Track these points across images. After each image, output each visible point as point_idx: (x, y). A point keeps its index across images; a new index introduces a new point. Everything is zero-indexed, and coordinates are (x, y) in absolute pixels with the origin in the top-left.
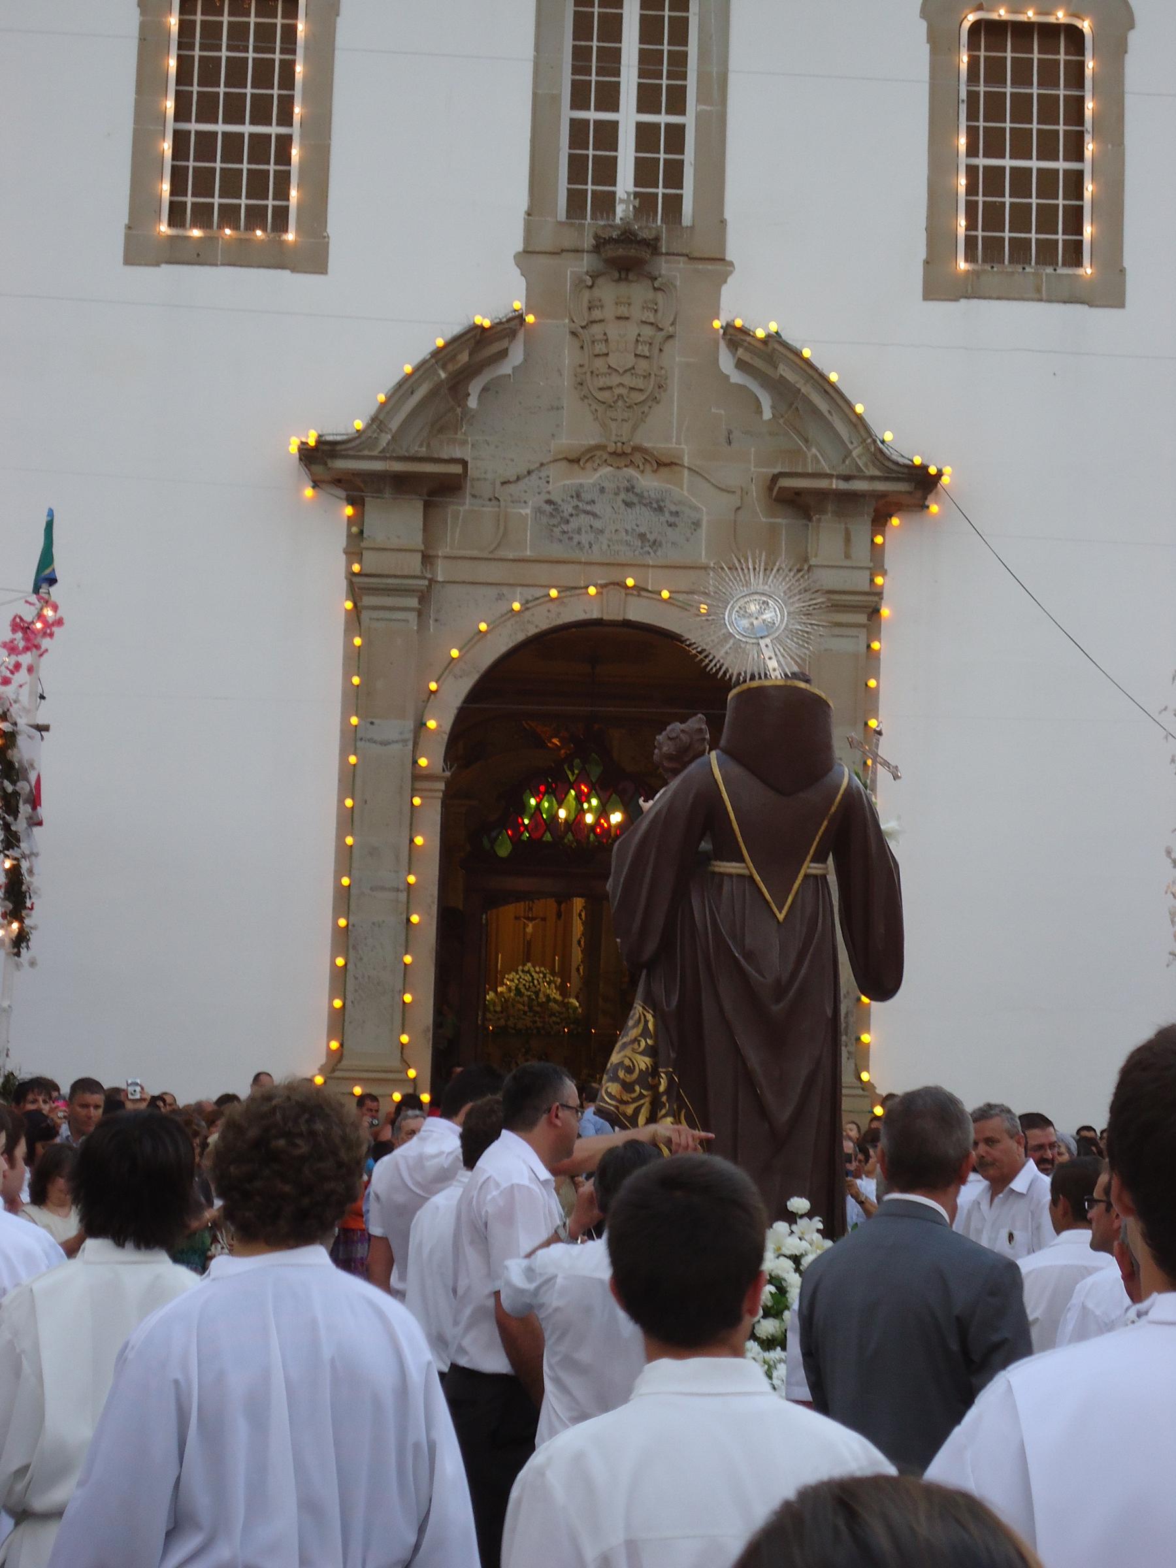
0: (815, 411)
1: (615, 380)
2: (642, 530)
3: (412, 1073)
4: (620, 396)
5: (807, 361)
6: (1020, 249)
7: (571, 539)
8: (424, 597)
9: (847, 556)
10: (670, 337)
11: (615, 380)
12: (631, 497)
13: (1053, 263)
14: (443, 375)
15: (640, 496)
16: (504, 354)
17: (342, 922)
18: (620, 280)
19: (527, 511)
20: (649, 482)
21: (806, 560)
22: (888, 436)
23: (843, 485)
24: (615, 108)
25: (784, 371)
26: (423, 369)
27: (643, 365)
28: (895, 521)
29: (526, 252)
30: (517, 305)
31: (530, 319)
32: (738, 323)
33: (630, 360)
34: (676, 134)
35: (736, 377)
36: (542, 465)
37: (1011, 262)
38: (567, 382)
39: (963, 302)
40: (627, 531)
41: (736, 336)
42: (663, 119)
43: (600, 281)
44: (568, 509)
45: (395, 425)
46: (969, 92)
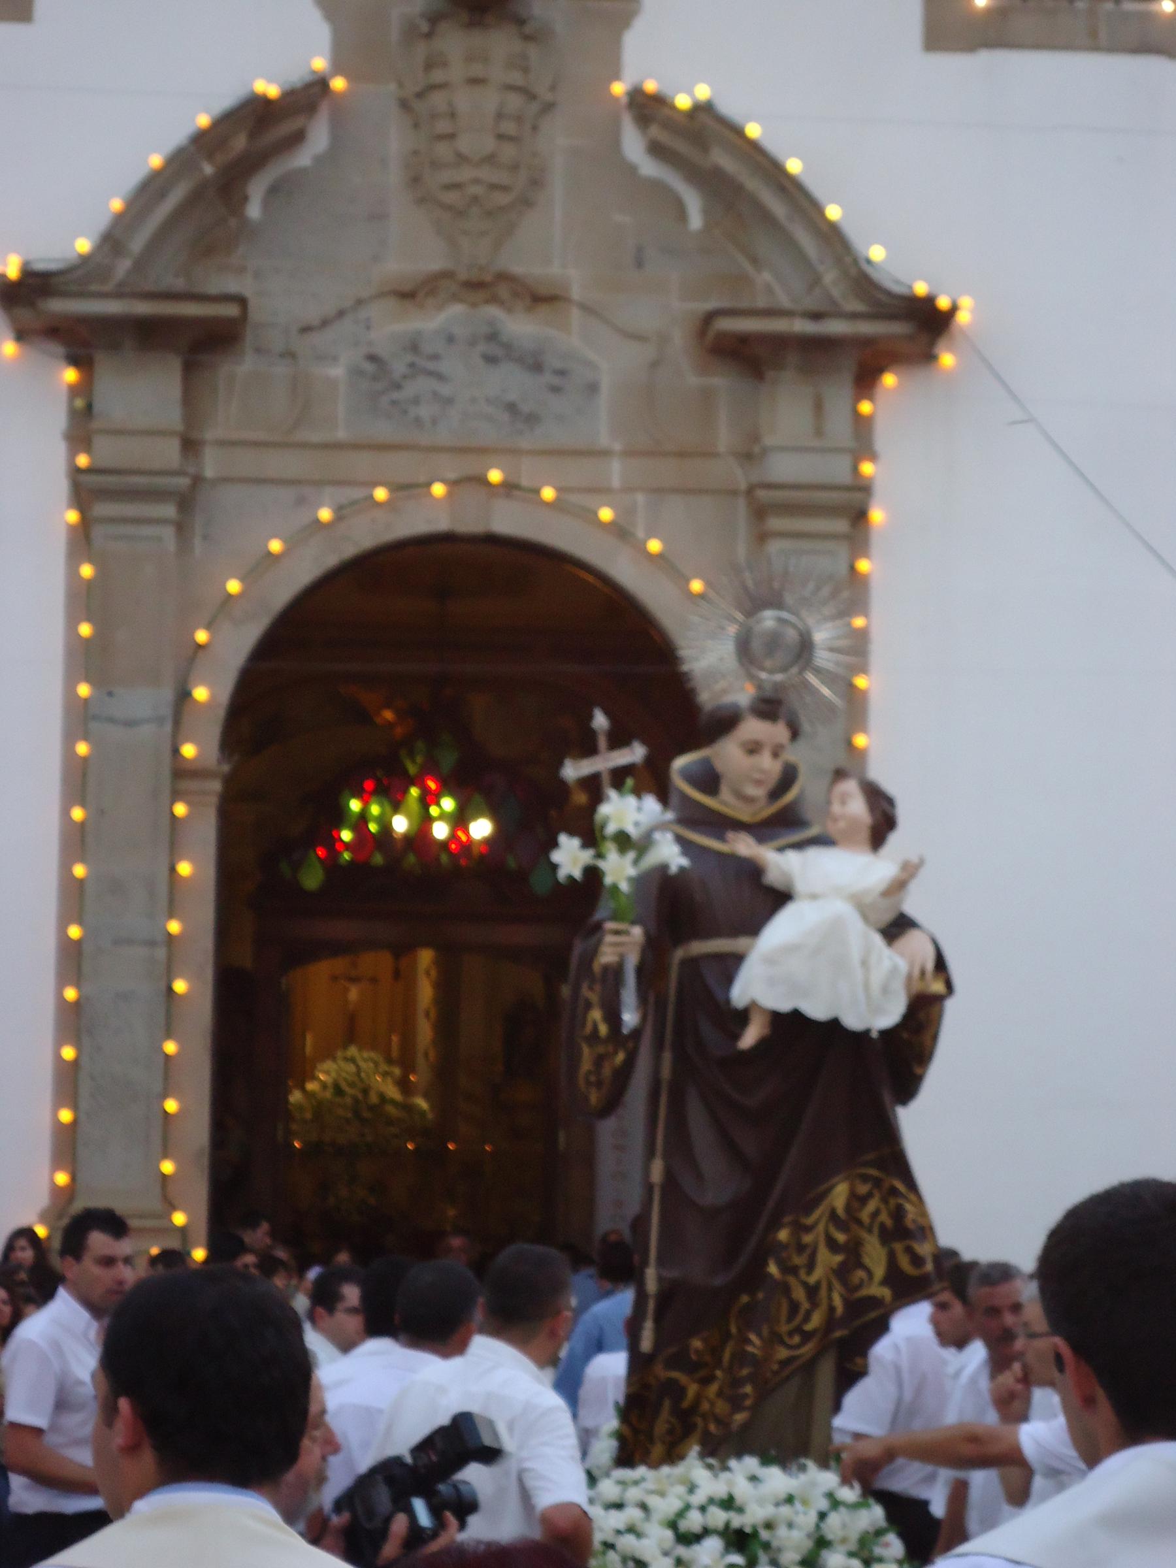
0: (766, 218)
1: (465, 174)
2: (512, 396)
3: (179, 1219)
4: (475, 199)
5: (754, 145)
7: (405, 412)
8: (186, 502)
9: (819, 432)
10: (549, 107)
11: (465, 174)
12: (494, 350)
15: (508, 347)
16: (297, 138)
17: (71, 994)
18: (471, 25)
19: (337, 372)
21: (755, 437)
22: (877, 253)
26: (179, 162)
27: (508, 152)
28: (889, 380)
30: (319, 64)
31: (338, 84)
32: (650, 86)
33: (489, 144)
35: (649, 167)
36: (360, 302)
38: (394, 177)
40: (488, 400)
43: (443, 26)
44: (399, 367)
45: (138, 243)
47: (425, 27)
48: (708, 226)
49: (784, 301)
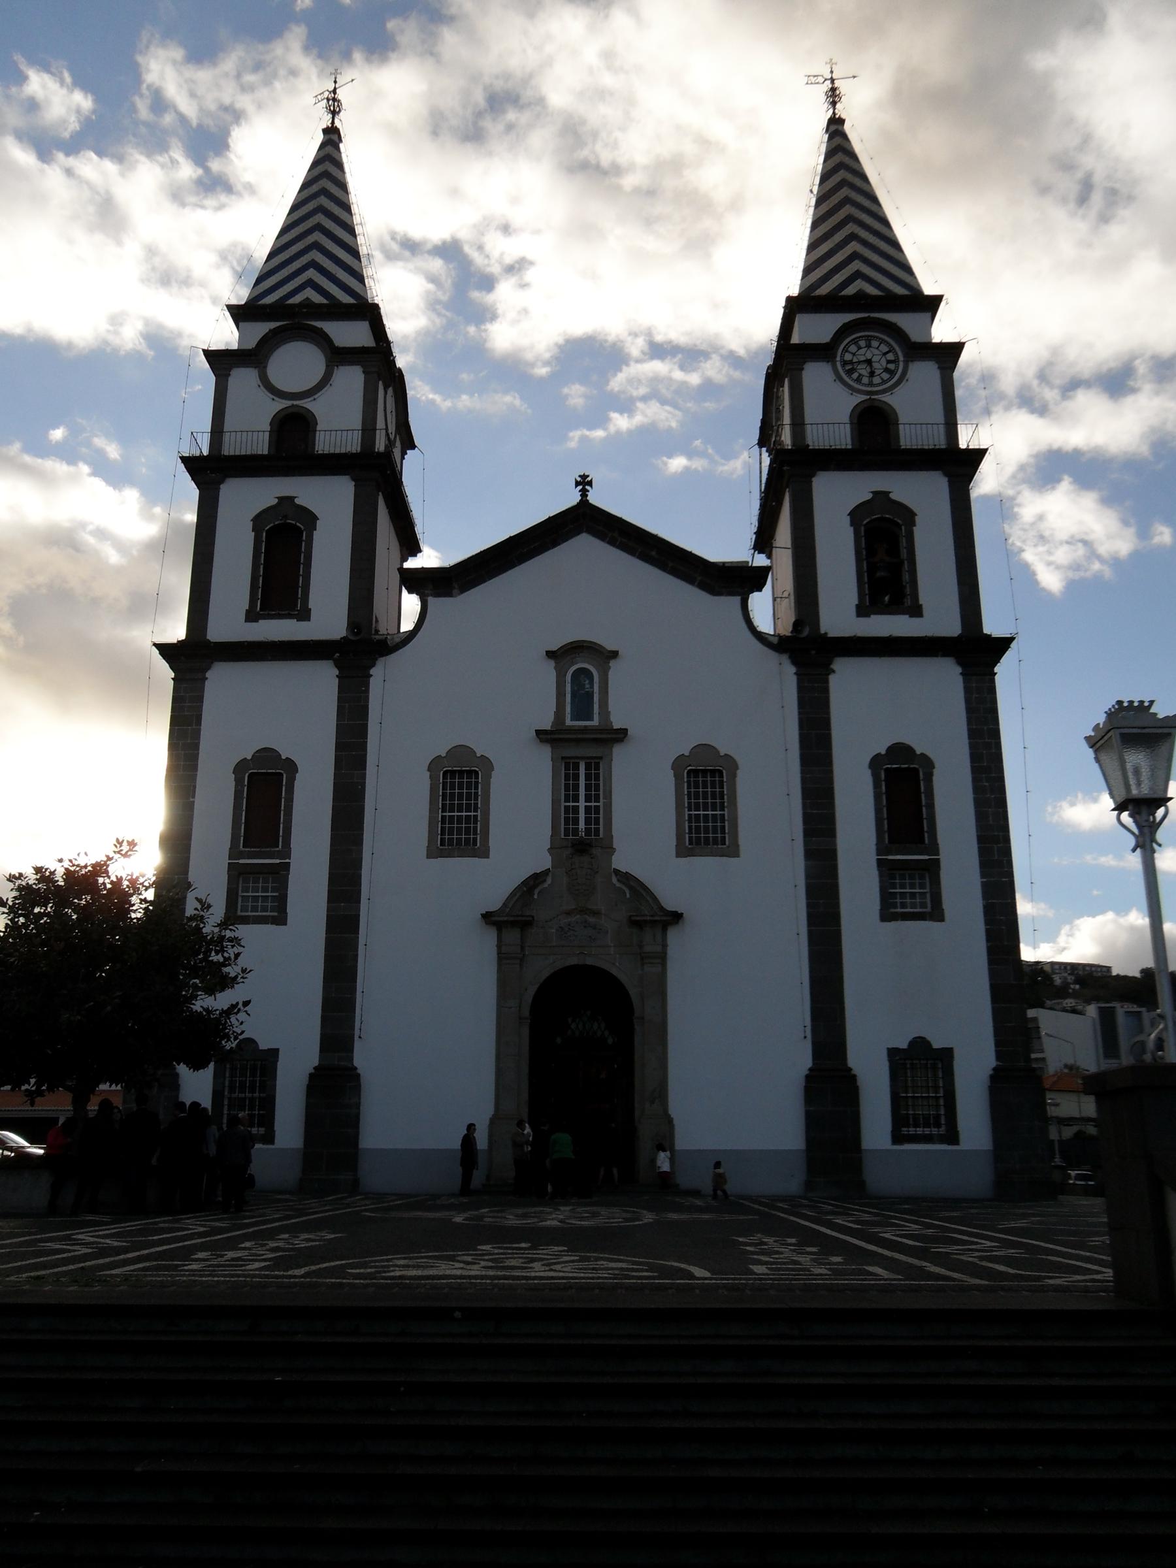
6: (707, 839)
10: (597, 872)
13: (717, 844)
14: (525, 889)
16: (545, 881)
20: (592, 920)
23: (651, 918)
24: (578, 802)
25: (632, 883)
29: (551, 848)
34: (598, 808)
35: (618, 885)
37: (705, 844)
39: (688, 858)
41: (617, 872)
42: (593, 804)
46: (688, 791)
47: (571, 856)
48: (630, 896)
49: (646, 912)
